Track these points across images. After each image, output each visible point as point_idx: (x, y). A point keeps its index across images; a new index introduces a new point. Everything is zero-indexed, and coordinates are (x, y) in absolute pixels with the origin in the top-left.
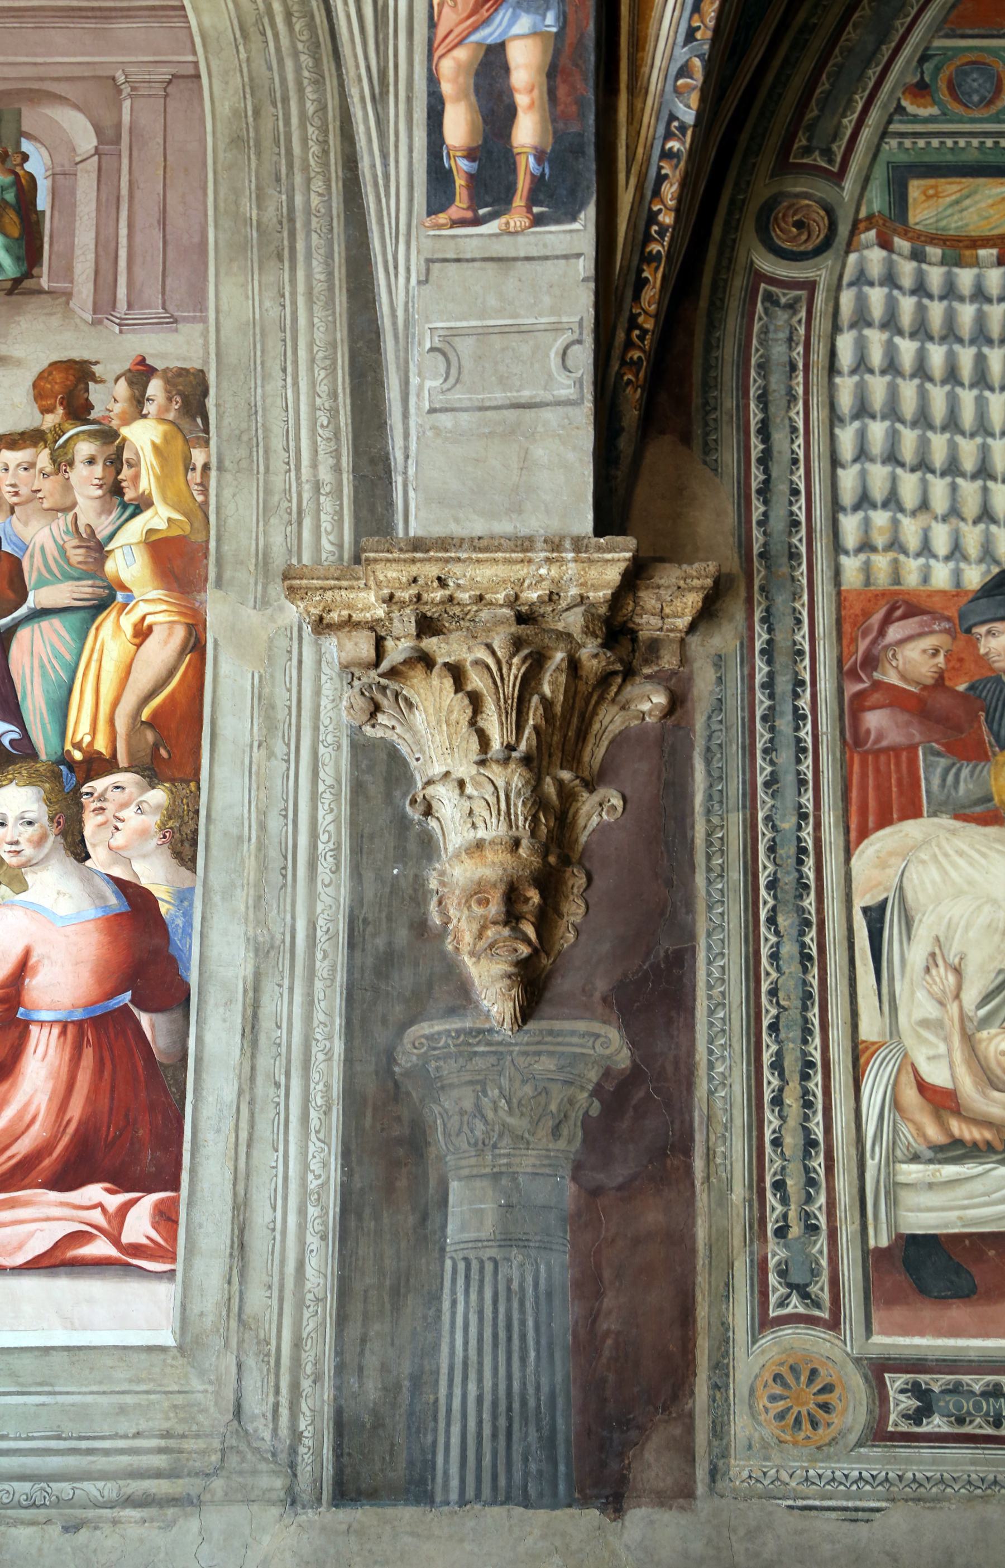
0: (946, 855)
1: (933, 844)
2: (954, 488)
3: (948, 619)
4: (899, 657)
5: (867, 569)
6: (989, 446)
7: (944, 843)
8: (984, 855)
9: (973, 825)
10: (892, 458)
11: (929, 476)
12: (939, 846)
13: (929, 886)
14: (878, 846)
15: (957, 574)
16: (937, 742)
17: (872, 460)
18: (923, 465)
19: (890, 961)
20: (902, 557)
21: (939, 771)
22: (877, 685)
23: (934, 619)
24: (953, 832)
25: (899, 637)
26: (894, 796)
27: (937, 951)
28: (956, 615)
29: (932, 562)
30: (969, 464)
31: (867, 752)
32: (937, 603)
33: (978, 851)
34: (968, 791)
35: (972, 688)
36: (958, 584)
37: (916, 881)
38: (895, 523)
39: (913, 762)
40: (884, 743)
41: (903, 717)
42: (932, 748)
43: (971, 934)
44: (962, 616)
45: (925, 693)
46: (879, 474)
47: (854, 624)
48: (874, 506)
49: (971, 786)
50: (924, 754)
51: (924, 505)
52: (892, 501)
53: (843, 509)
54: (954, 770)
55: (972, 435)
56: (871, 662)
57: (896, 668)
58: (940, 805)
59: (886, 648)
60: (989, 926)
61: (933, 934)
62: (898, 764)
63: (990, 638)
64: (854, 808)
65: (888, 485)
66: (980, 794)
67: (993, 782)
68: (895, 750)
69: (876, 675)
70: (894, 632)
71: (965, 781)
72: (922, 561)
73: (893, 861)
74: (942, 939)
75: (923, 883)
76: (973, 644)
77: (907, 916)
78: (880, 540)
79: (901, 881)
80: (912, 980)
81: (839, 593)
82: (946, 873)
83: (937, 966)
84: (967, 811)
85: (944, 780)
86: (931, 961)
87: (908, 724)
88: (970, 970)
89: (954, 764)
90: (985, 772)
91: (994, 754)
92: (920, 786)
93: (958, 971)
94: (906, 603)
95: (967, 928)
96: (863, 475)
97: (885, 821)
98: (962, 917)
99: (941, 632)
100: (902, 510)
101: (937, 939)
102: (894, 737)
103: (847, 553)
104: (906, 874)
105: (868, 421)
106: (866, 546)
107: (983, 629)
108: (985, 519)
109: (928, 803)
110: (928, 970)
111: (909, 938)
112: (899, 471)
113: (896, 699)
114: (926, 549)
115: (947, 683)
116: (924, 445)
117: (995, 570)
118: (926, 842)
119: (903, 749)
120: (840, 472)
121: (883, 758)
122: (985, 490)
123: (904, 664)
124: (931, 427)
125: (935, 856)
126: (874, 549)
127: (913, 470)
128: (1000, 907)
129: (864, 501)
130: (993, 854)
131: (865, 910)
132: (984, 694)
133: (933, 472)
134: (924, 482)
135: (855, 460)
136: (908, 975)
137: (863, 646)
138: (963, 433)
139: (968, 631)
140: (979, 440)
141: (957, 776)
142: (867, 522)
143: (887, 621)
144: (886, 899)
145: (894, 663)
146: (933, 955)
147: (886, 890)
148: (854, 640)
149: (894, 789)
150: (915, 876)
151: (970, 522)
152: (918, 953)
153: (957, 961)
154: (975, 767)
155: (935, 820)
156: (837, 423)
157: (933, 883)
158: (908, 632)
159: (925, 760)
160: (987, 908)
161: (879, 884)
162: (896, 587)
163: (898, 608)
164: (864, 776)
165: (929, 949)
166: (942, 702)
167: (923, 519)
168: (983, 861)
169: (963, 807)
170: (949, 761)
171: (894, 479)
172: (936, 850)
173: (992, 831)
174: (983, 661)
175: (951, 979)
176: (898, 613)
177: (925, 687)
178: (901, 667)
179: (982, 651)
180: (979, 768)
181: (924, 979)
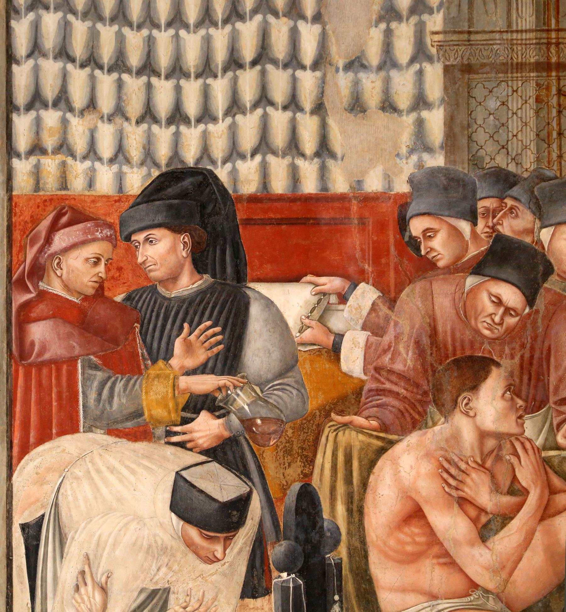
0: (98, 471)
1: (88, 459)
2: (120, 85)
3: (110, 226)
4: (63, 266)
5: (37, 173)
6: (155, 38)
7: (97, 459)
8: (133, 472)
9: (124, 441)
10: (63, 53)
11: (97, 72)
12: (92, 461)
13: (82, 503)
14: (31, 465)
15: (120, 178)
16: (94, 354)
17: (45, 55)
18: (92, 61)
19: (44, 580)
20: (69, 160)
21: (96, 384)
22: (42, 295)
23: (97, 226)
24: (106, 448)
25: (64, 245)
26: (54, 410)
27: (87, 569)
28: (117, 222)
29: (97, 165)
30: (135, 59)
31: (30, 365)
32: (100, 209)
33: (127, 467)
34: (121, 405)
35: (128, 298)
36: (120, 189)
37: (70, 498)
38: (65, 122)
39: (72, 375)
40: (47, 356)
41: (65, 329)
42: (90, 360)
43: (118, 552)
44: (122, 223)
45: (85, 304)
46: (51, 68)
47: (23, 231)
48: (45, 106)
49: (124, 401)
50: (83, 367)
51: (92, 104)
52: (62, 100)
53: (17, 109)
54: (109, 384)
55: (140, 27)
56: (38, 271)
57: (60, 277)
58: (95, 420)
59: (52, 256)
60: (135, 544)
61: (83, 552)
62: (58, 377)
63: (147, 246)
64: (17, 423)
65: (59, 82)
66: (131, 409)
67: (144, 397)
68: (56, 363)
69: (42, 285)
70: (61, 240)
71: (119, 395)
72: (88, 164)
73: (50, 477)
74: (91, 557)
75: (77, 501)
76: (132, 252)
77: (60, 534)
78: (50, 142)
79: (57, 497)
80: (62, 598)
81: (10, 199)
82: (98, 490)
83: (86, 584)
84: (120, 426)
85: (100, 394)
86: (80, 579)
87: (69, 336)
88: (115, 588)
89: (109, 378)
90: (137, 386)
91: (147, 367)
92: (77, 401)
93: (104, 590)
94: (73, 209)
95: (115, 545)
96: (36, 70)
97: (44, 437)
98: (110, 534)
99: (102, 239)
100: (71, 109)
101: (87, 557)
102: (56, 350)
103: (18, 156)
104: (62, 490)
105: (42, 12)
106: (37, 149)
107: (140, 237)
108: (148, 118)
109: (85, 418)
110: (77, 588)
111: (62, 557)
112: (70, 66)
113: (60, 310)
114: (92, 151)
115: (107, 293)
116: (94, 37)
117: (156, 173)
118: (81, 458)
119: (64, 362)
120: (15, 67)
121: (45, 371)
122: (149, 87)
123: (68, 273)
124: (101, 19)
125: (89, 472)
126: (44, 152)
127: (82, 66)
128: (145, 524)
129: (37, 100)
130: (140, 470)
131: (24, 527)
132: (140, 305)
133: (101, 68)
134: (92, 77)
135: (29, 56)
136: (59, 593)
137: (31, 254)
138: (130, 25)
139: (128, 239)
140: (145, 32)
141: (112, 389)
142: (38, 122)
143: (54, 228)
144: (43, 516)
145: (59, 272)
146: (83, 573)
147: (43, 506)
148: (23, 249)
149: (54, 404)
150: (69, 493)
151: (134, 121)
152: (68, 572)
153: (103, 579)
154: (128, 381)
155: (90, 435)
156: (13, 14)
157: (86, 500)
158: (73, 240)
159: (83, 373)
160: (133, 526)
161: (37, 500)
162: (63, 192)
163: (65, 214)
164: (27, 389)
165: (79, 567)
166: (101, 312)
167: (90, 118)
168: (132, 478)
169: (116, 422)
170: (106, 375)
171: (65, 76)
172: (90, 465)
173: (141, 446)
174: (140, 270)
175: (98, 597)
176: (64, 219)
177: (86, 298)
178: (64, 277)
179: (140, 260)
180: (132, 382)
181: (73, 598)
